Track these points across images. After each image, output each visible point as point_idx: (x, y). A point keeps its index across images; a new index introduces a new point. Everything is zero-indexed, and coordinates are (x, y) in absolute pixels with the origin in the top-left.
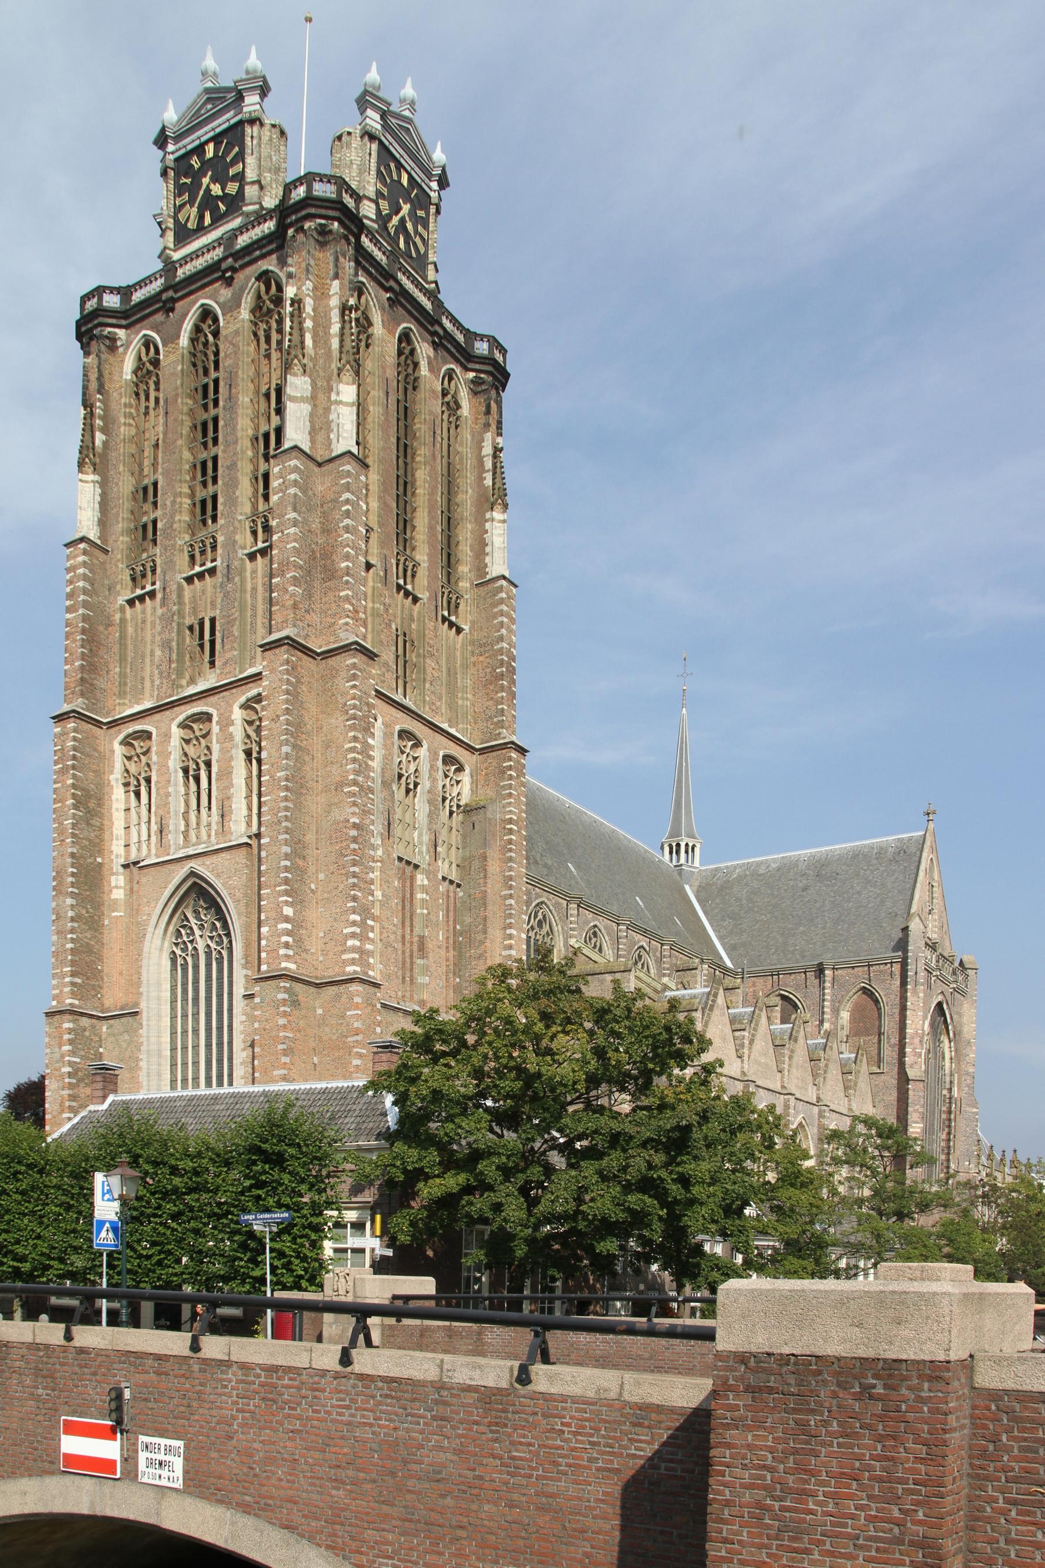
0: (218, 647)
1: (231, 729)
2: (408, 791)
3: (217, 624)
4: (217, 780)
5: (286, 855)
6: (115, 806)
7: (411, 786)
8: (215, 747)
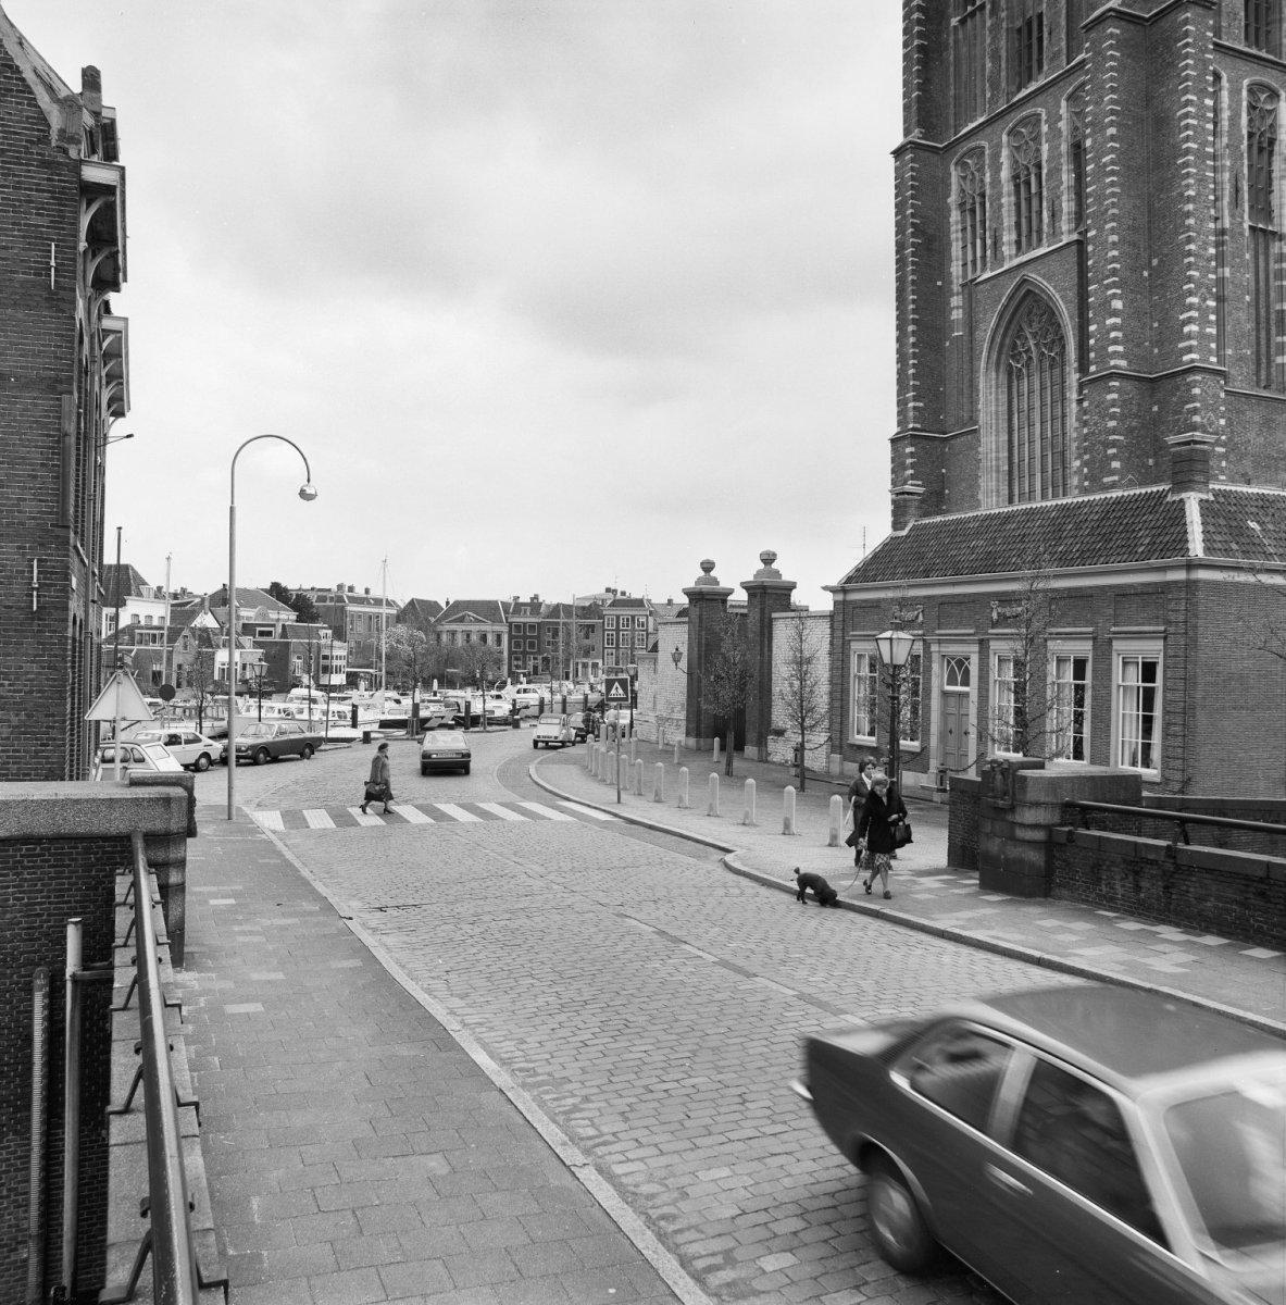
0: (1045, 43)
1: (1060, 124)
2: (1261, 150)
3: (1045, 19)
4: (1047, 180)
5: (1114, 243)
6: (953, 228)
7: (1265, 145)
8: (1045, 147)
